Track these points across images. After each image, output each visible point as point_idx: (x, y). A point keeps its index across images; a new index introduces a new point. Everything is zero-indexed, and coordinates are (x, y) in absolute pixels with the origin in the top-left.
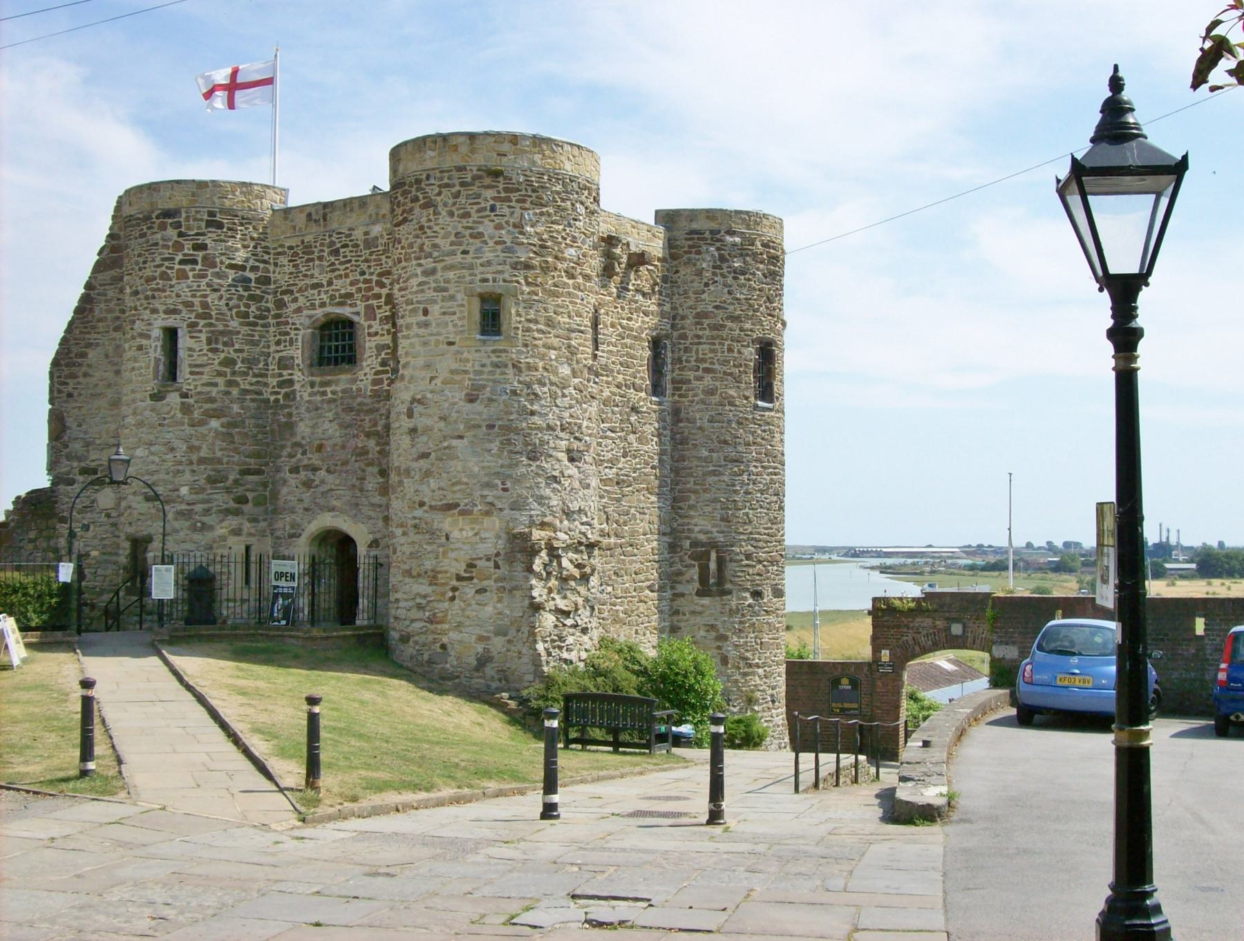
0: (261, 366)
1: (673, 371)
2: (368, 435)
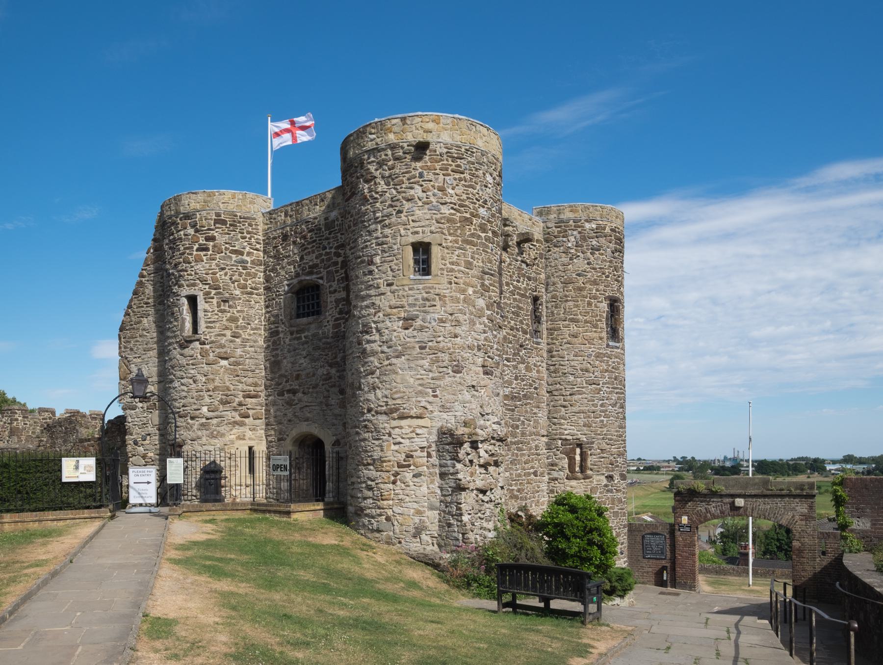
0: (256, 322)
1: (547, 322)
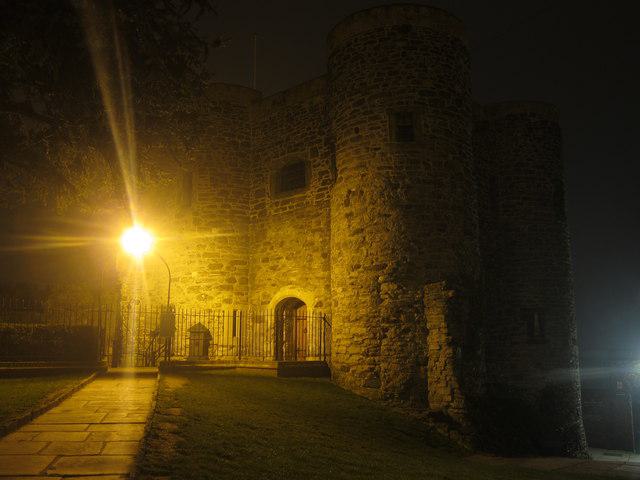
2: (314, 231)
